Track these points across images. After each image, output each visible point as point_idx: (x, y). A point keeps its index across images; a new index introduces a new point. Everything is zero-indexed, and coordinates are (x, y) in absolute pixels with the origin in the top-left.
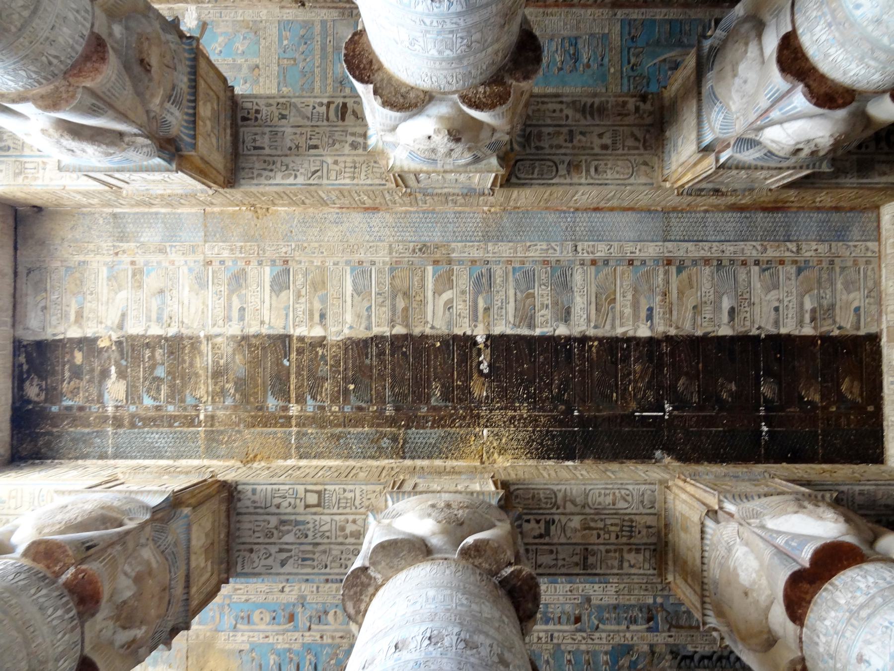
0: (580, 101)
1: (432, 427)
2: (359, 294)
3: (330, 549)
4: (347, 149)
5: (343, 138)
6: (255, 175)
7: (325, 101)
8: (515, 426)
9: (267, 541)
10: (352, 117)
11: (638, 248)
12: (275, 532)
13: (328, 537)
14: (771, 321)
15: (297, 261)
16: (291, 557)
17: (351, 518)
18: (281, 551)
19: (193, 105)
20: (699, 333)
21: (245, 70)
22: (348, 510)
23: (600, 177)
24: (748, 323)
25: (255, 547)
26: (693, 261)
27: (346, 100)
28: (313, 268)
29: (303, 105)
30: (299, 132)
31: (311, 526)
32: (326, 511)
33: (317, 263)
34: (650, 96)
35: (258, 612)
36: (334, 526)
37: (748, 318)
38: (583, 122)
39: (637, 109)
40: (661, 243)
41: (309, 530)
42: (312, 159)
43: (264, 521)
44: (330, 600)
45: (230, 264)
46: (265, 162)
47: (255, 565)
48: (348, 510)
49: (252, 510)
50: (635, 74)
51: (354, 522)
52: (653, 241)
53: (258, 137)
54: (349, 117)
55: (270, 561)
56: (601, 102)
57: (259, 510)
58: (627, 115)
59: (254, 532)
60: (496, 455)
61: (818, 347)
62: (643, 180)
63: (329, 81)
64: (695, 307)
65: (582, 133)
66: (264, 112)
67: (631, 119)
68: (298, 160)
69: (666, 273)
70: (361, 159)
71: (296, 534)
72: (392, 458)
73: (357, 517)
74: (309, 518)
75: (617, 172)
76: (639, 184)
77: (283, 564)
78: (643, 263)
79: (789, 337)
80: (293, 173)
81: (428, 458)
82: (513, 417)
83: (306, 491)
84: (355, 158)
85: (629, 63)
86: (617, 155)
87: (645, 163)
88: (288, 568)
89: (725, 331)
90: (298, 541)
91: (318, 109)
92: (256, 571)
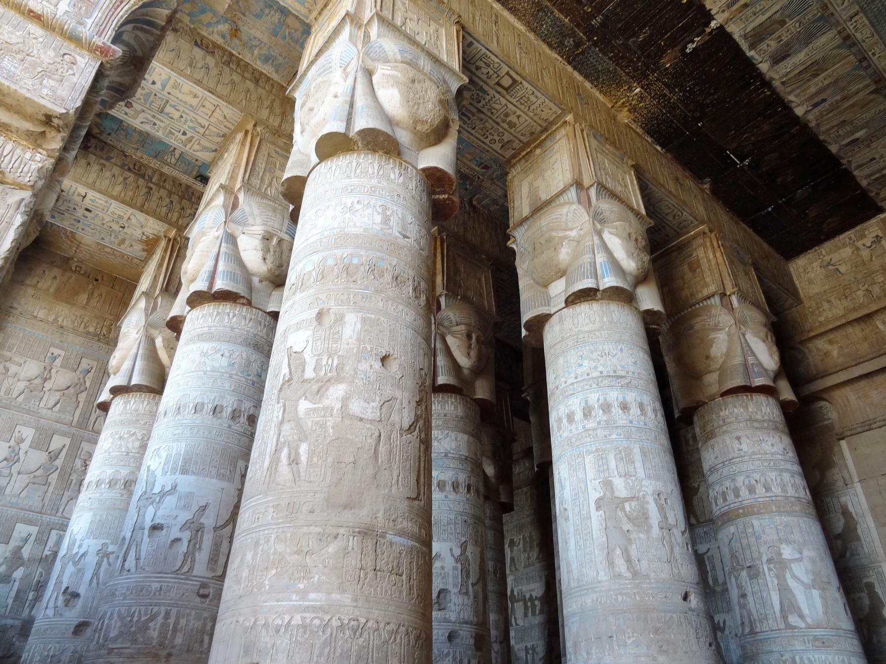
1: (610, 59)
3: (487, 121)
8: (659, 102)
13: (492, 113)
17: (519, 112)
22: (522, 107)
31: (488, 98)
32: (508, 97)
36: (503, 109)
48: (522, 107)
51: (519, 117)
60: (626, 109)
71: (473, 95)
72: (562, 57)
73: (524, 115)
74: (492, 92)
81: (585, 77)
82: (665, 95)
83: (508, 74)
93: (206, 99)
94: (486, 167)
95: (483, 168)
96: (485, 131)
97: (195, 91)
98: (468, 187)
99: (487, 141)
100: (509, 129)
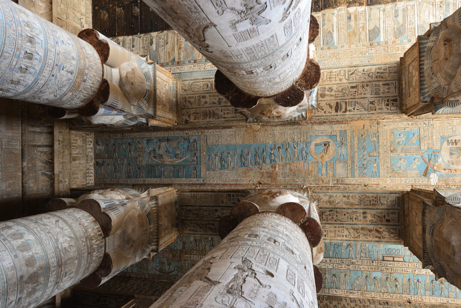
0: (216, 119)
2: (330, 32)
4: (335, 87)
5: (337, 93)
6: (388, 69)
7: (348, 113)
10: (332, 105)
11: (192, 69)
14: (135, 41)
15: (365, 46)
19: (421, 63)
20: (165, 32)
21: (399, 149)
23: (206, 82)
24: (145, 39)
26: (168, 65)
27: (336, 114)
28: (355, 43)
29: (360, 110)
30: (362, 95)
33: (353, 46)
34: (184, 123)
37: (145, 41)
38: (214, 109)
39: (189, 117)
40: (182, 72)
42: (354, 81)
45: (405, 41)
46: (382, 77)
50: (194, 152)
52: (186, 72)
53: (387, 90)
54: (334, 104)
56: (206, 119)
58: (194, 113)
61: (117, 31)
62: (186, 83)
63: (349, 144)
64: (167, 43)
65: (214, 103)
66: (383, 105)
67: (192, 111)
68: (363, 80)
69: (179, 58)
70: (326, 83)
75: (198, 85)
76: (188, 80)
78: (190, 62)
79: (128, 35)
80: (365, 72)
84: (330, 83)
85: (197, 157)
86: (198, 94)
87: (185, 90)
89: (154, 34)
91: (352, 108)
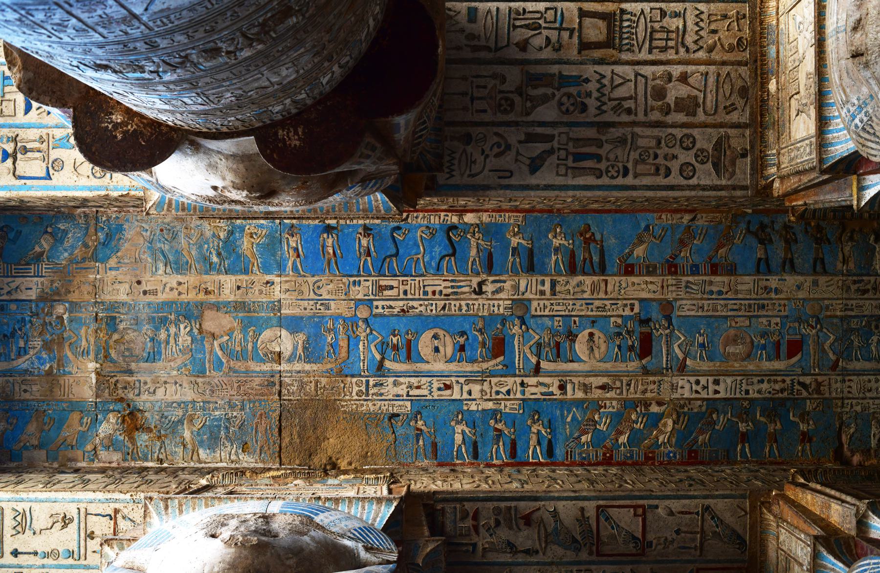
3: (634, 135)
9: (501, 117)
12: (517, 99)
13: (629, 111)
16: (551, 152)
17: (676, 70)
18: (531, 138)
25: (475, 131)
31: (592, 86)
32: (626, 56)
35: (429, 334)
41: (589, 95)
43: (494, 76)
44: (580, 309)
47: (476, 168)
48: (671, 55)
49: (467, 54)
55: (507, 161)
57: (483, 55)
59: (472, 99)
71: (561, 104)
74: (590, 70)
77: (535, 166)
88: (545, 176)
90: (565, 119)
92: (478, 180)
93: (87, 514)
94: (795, 347)
95: (790, 356)
96: (651, 161)
97: (59, 508)
98: (803, 427)
99: (675, 179)
100: (690, 119)
